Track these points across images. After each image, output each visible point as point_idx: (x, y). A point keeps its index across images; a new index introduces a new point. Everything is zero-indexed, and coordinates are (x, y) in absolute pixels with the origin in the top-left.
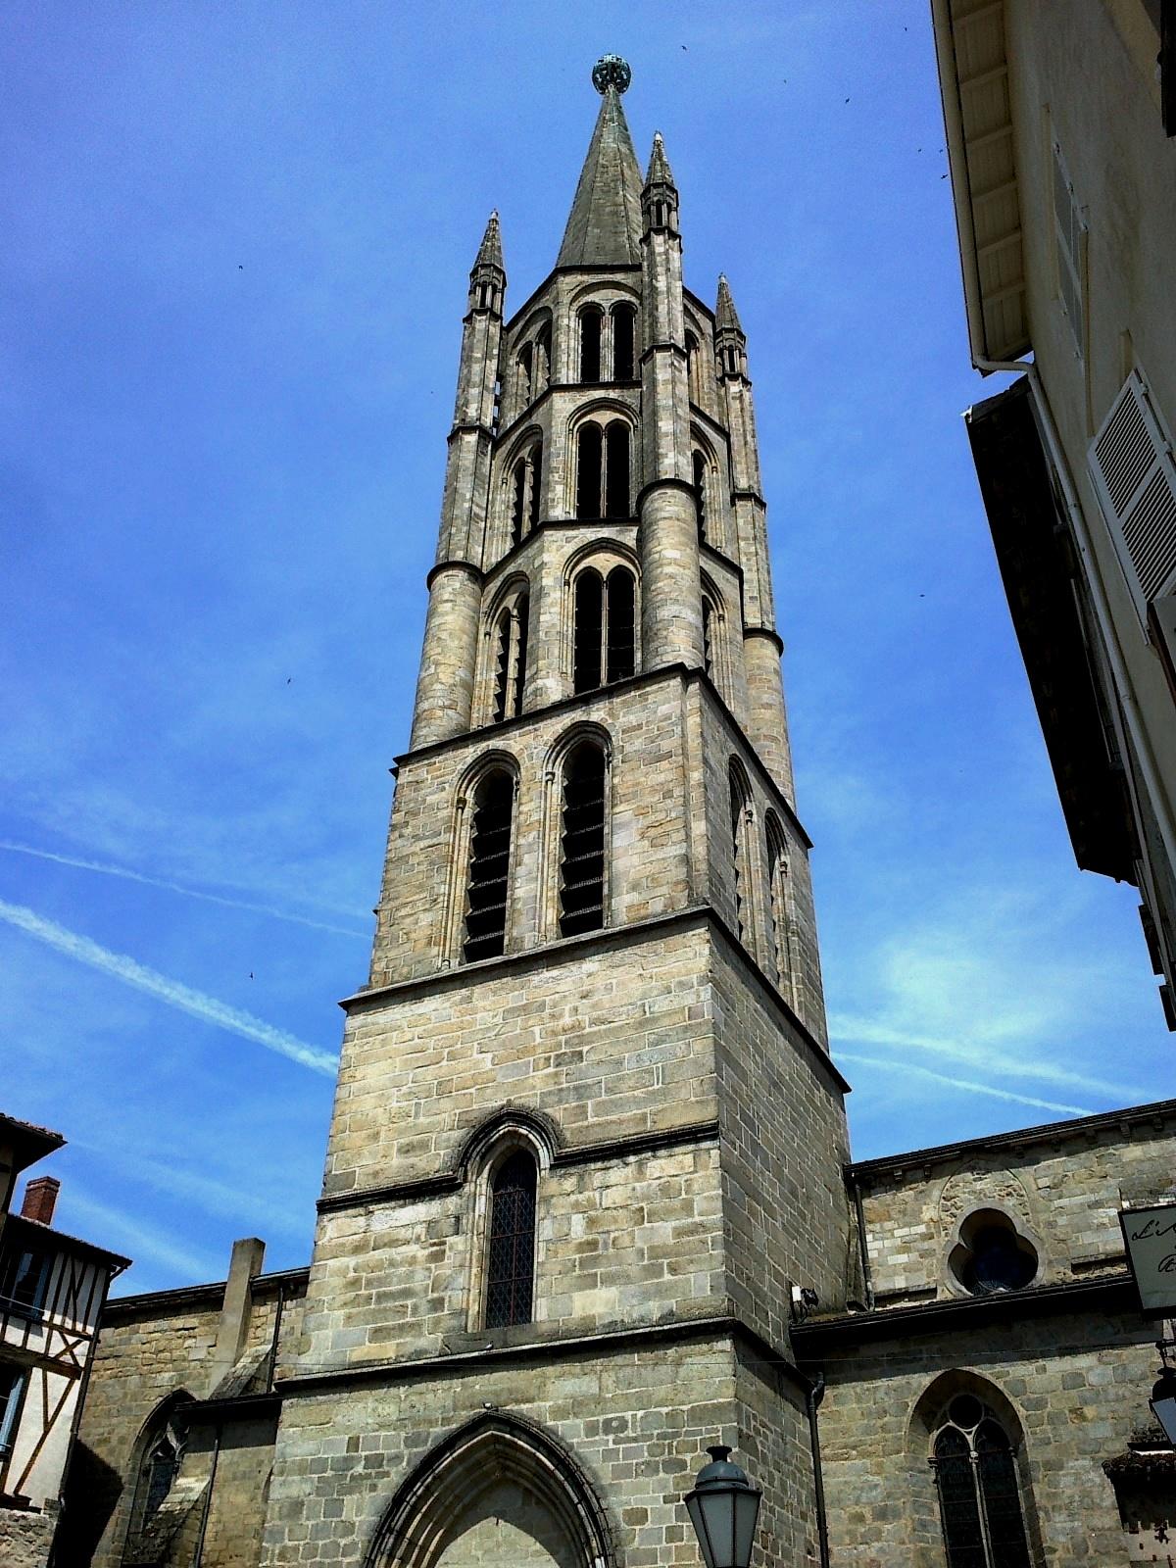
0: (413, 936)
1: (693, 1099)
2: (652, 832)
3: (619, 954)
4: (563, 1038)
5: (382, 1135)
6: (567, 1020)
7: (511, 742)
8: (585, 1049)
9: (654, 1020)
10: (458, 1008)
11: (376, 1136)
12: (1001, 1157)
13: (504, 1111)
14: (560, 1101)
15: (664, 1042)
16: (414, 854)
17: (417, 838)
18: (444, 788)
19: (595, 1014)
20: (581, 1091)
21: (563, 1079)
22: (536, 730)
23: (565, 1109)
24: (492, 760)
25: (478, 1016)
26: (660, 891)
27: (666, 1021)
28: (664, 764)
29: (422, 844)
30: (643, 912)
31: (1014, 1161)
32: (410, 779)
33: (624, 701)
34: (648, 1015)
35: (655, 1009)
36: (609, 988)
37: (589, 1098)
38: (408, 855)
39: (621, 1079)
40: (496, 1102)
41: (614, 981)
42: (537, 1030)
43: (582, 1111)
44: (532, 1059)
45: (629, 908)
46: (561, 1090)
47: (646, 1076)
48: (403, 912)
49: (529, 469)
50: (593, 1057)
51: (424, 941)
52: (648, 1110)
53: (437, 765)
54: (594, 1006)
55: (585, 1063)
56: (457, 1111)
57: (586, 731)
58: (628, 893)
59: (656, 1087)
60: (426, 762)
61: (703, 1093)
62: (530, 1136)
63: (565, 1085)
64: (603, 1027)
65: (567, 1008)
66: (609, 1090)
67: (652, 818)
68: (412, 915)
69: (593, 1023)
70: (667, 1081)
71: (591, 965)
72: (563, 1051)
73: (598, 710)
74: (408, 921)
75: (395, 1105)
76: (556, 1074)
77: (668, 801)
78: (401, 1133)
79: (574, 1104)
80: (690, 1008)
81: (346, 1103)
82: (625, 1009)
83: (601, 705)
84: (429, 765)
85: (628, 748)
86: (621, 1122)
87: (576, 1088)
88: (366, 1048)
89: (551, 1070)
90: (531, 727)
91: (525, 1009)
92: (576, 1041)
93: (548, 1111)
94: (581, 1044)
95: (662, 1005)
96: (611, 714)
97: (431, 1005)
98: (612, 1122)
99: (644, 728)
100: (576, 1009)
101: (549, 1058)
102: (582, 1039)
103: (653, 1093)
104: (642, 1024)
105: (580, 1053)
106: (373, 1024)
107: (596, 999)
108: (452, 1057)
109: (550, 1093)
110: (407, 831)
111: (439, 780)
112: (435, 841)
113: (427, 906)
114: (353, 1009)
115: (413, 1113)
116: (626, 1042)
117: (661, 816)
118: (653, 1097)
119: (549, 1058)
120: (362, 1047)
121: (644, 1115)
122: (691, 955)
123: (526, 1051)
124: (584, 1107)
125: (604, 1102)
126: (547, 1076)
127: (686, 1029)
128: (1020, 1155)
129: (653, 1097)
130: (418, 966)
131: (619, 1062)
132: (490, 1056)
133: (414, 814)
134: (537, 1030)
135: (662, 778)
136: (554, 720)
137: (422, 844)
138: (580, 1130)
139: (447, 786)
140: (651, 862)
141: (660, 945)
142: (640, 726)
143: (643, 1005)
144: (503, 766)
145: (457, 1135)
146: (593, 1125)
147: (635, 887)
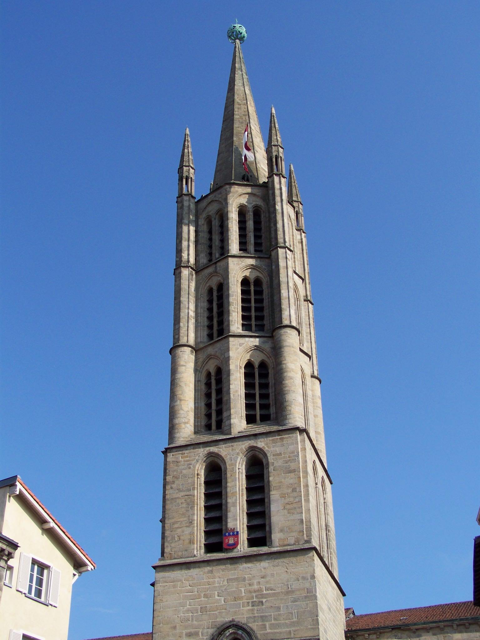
0: (182, 538)
1: (309, 627)
2: (288, 507)
3: (277, 561)
4: (254, 595)
5: (178, 627)
6: (256, 587)
7: (221, 450)
8: (264, 600)
9: (292, 592)
10: (207, 575)
11: (175, 628)
12: (407, 633)
13: (232, 623)
14: (254, 622)
15: (296, 601)
16: (178, 498)
17: (179, 490)
18: (190, 468)
19: (268, 586)
20: (263, 618)
21: (255, 612)
22: (232, 446)
23: (257, 625)
24: (211, 456)
25: (216, 580)
26: (292, 534)
27: (298, 593)
28: (292, 475)
29: (182, 494)
30: (286, 543)
31: (412, 634)
32: (173, 460)
33: (273, 440)
34: (290, 589)
35: (293, 587)
36: (272, 575)
37: (267, 621)
38: (176, 498)
39: (279, 615)
40: (228, 619)
41: (275, 572)
42: (243, 590)
43: (264, 627)
44: (241, 602)
45: (280, 540)
46: (255, 617)
47: (290, 615)
48: (176, 526)
49: (215, 294)
50: (268, 604)
51: (187, 541)
52: (291, 629)
53: (186, 454)
54: (267, 582)
55: (264, 606)
56: (211, 621)
57: (256, 450)
58: (278, 533)
59: (294, 620)
60: (181, 452)
61: (314, 625)
62: (243, 635)
63: (256, 615)
64: (271, 592)
65: (255, 582)
66: (275, 619)
67: (287, 500)
68: (181, 528)
69: (267, 589)
70: (299, 617)
71: (265, 564)
72: (255, 600)
73: (261, 442)
74: (179, 530)
75: (182, 615)
76: (253, 610)
77: (295, 493)
78: (186, 627)
79: (260, 623)
80: (307, 589)
81: (159, 612)
82: (280, 585)
83: (262, 440)
84: (182, 454)
85: (276, 464)
86: (280, 633)
87: (262, 617)
88: (166, 587)
89: (250, 608)
90: (230, 444)
91: (237, 579)
92: (260, 596)
93: (250, 625)
94: (262, 598)
95: (295, 585)
96: (267, 444)
97: (194, 572)
98: (278, 633)
99: (283, 455)
100: (259, 583)
101: (248, 603)
102: (263, 596)
103: (293, 622)
104: (288, 593)
105: (262, 602)
106: (168, 577)
107: (268, 579)
108: (206, 596)
109: (250, 617)
110: (174, 486)
111: (188, 462)
112: (188, 493)
113: (187, 525)
114: (158, 569)
115: (191, 619)
116: (281, 599)
117: (292, 499)
118: (293, 624)
119: (248, 603)
120: (164, 587)
121: (290, 632)
122: (307, 565)
123: (241, 598)
124: (265, 625)
125: (273, 624)
126: (249, 610)
127: (306, 597)
128: (414, 632)
129: (293, 624)
130: (186, 552)
131: (279, 608)
132: (223, 599)
133: (177, 478)
134: (243, 590)
135: (291, 481)
136: (240, 443)
137: (182, 494)
138: (264, 634)
139: (191, 466)
140: (288, 520)
141: (294, 559)
142: (280, 454)
143: (288, 585)
144: (216, 460)
145: (211, 631)
146: (269, 633)
147: (282, 531)
